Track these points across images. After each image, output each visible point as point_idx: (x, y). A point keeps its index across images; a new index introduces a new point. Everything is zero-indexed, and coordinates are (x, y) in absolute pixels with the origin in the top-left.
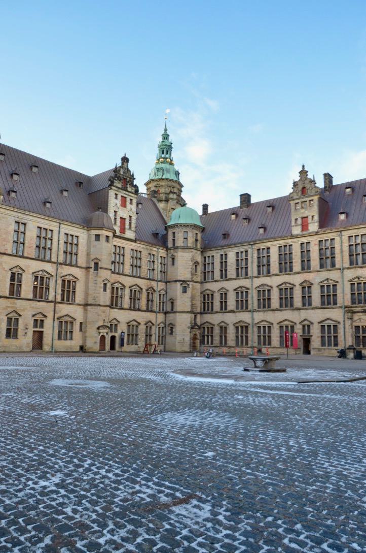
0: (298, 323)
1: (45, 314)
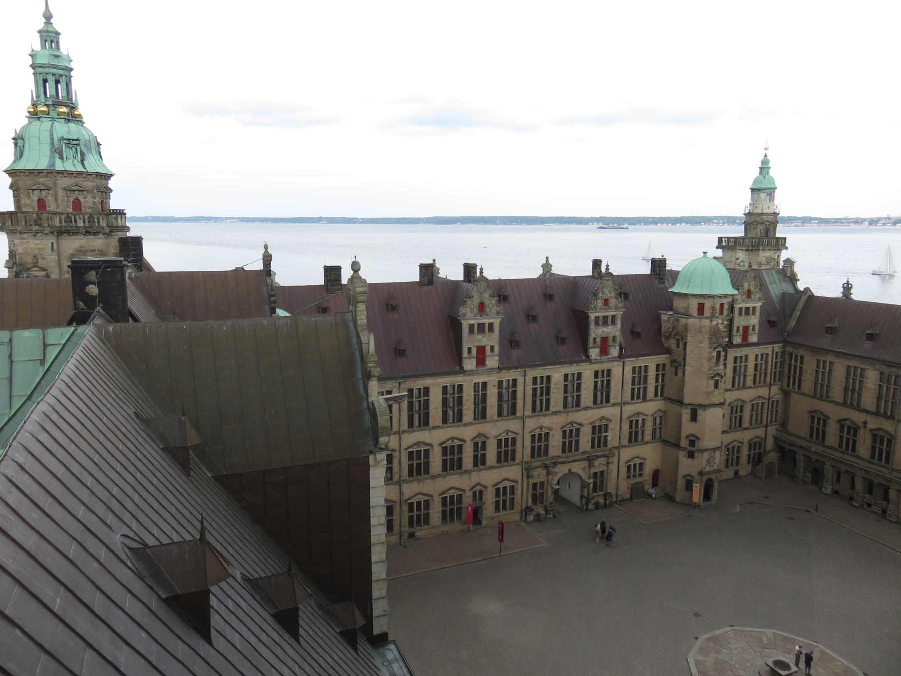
0: (467, 489)
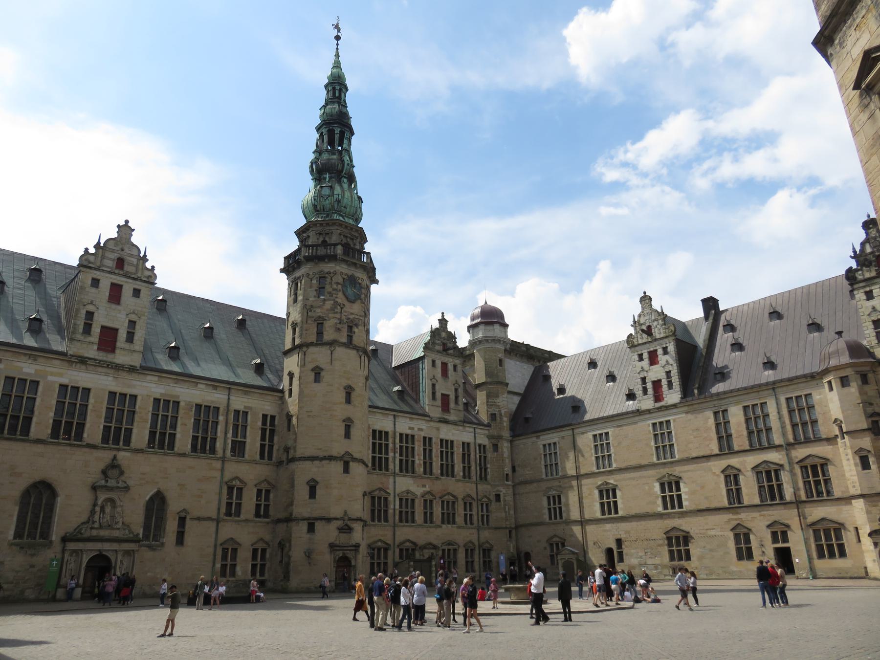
1: (786, 522)
